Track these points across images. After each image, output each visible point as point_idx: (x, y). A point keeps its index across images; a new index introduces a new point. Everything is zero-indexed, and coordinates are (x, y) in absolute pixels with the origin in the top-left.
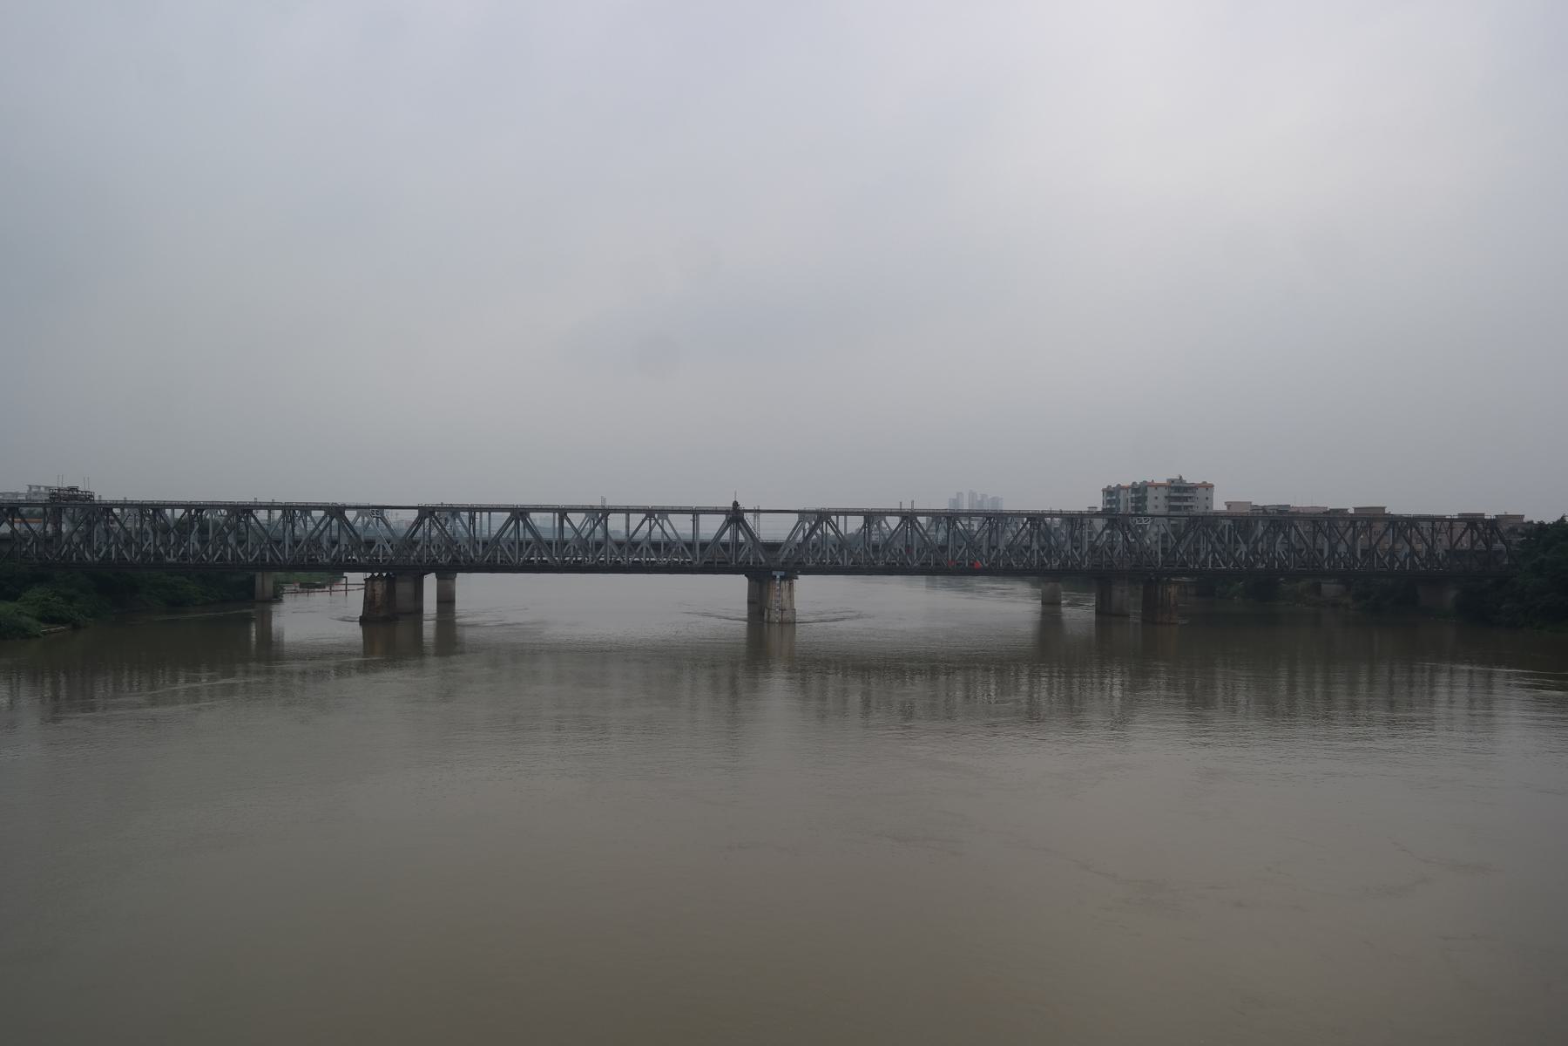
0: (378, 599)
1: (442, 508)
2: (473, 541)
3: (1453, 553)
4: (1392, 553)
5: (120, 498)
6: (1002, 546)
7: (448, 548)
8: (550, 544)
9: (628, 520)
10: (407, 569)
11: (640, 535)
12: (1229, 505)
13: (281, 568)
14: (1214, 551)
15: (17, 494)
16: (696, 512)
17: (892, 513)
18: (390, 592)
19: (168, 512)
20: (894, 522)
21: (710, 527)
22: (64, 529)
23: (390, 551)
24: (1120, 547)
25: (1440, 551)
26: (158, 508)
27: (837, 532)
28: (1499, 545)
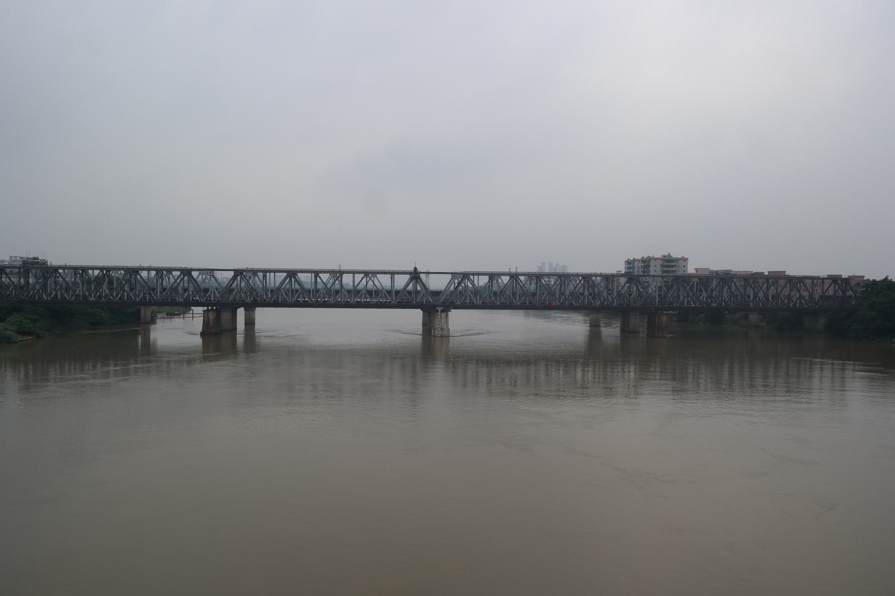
0: (211, 322)
1: (248, 271)
2: (265, 289)
3: (824, 297)
4: (789, 297)
5: (62, 263)
6: (567, 293)
7: (251, 293)
8: (309, 291)
9: (354, 278)
10: (227, 305)
11: (361, 287)
12: (697, 270)
14: (688, 296)
15: (3, 261)
16: (393, 273)
17: (505, 274)
18: (218, 318)
19: (90, 272)
20: (506, 279)
21: (401, 282)
22: (31, 281)
23: (218, 295)
24: (634, 294)
25: (816, 296)
26: (85, 270)
27: (473, 285)
28: (850, 293)
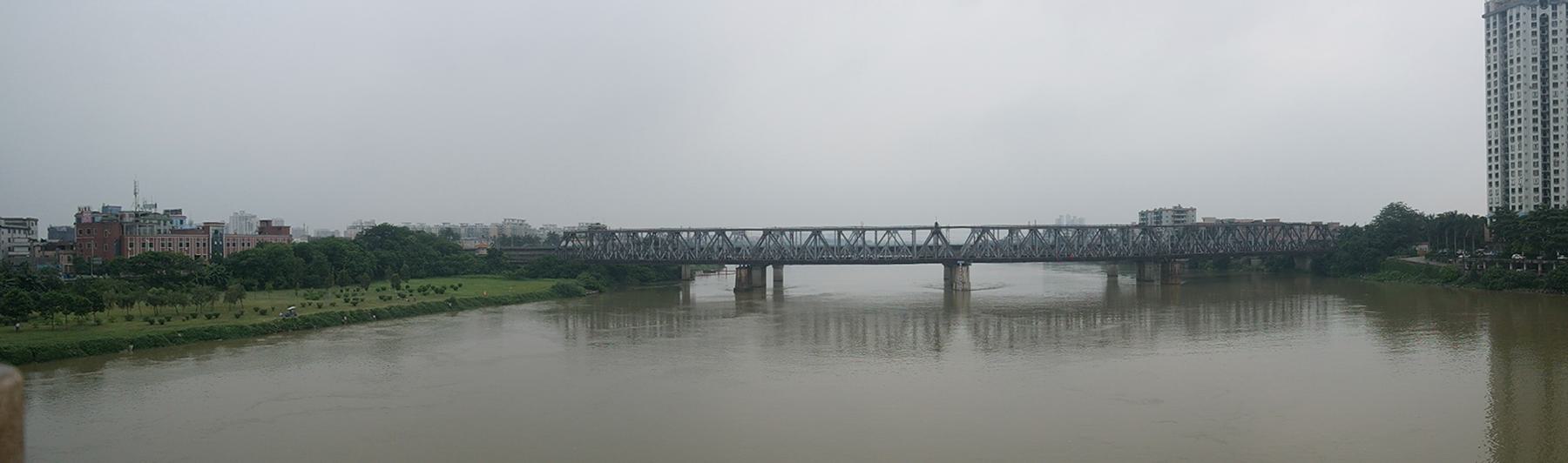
3: (1310, 241)
4: (1283, 242)
10: (757, 262)
16: (913, 229)
18: (749, 274)
20: (1025, 232)
21: (922, 237)
26: (635, 232)
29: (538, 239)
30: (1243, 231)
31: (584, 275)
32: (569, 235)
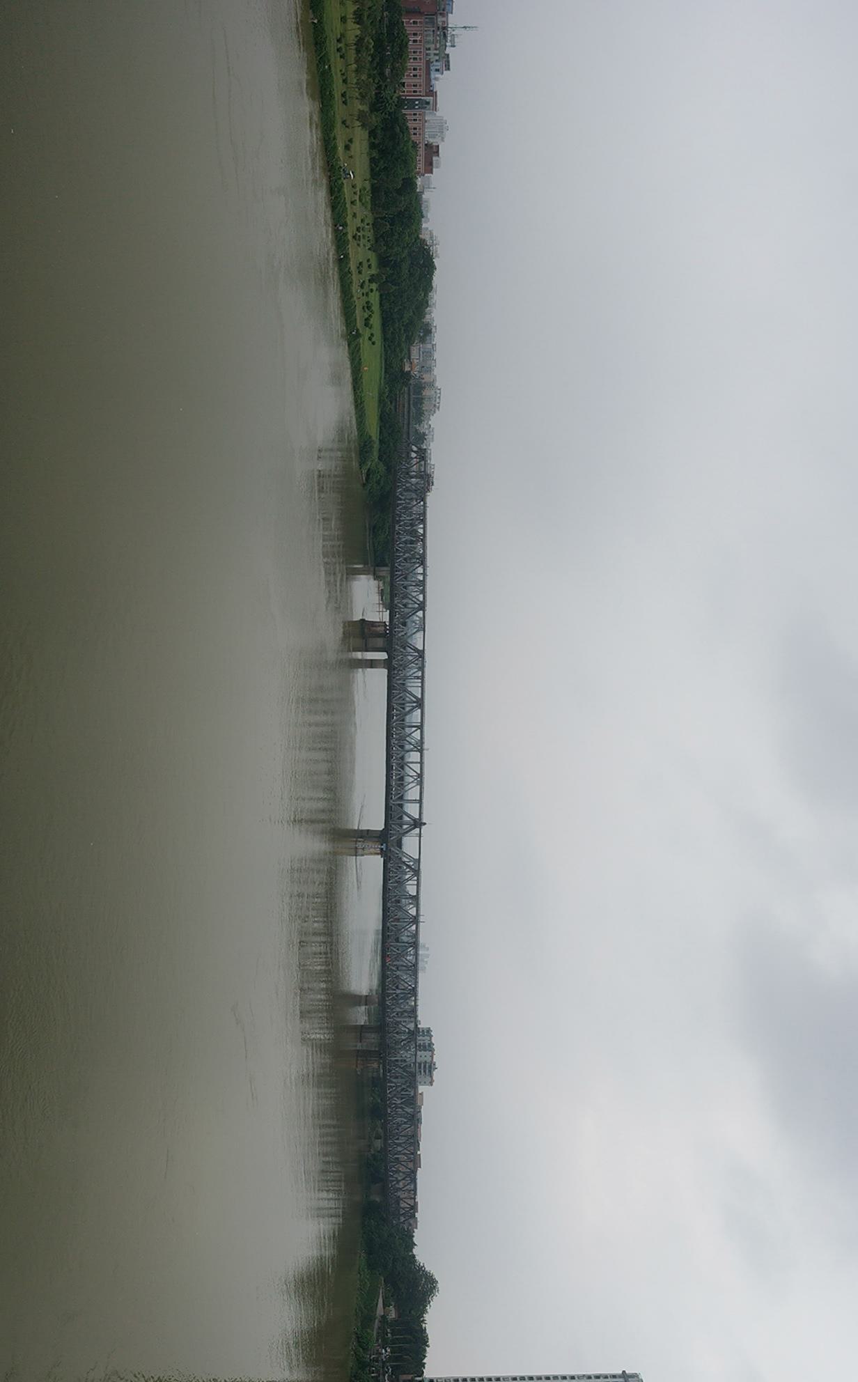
2: (405, 678)
3: (398, 1200)
4: (398, 1171)
10: (390, 644)
13: (392, 580)
16: (420, 801)
18: (379, 635)
20: (413, 912)
21: (412, 810)
25: (399, 1194)
26: (423, 521)
28: (402, 1219)
29: (420, 422)
30: (409, 1131)
31: (382, 468)
32: (423, 455)
